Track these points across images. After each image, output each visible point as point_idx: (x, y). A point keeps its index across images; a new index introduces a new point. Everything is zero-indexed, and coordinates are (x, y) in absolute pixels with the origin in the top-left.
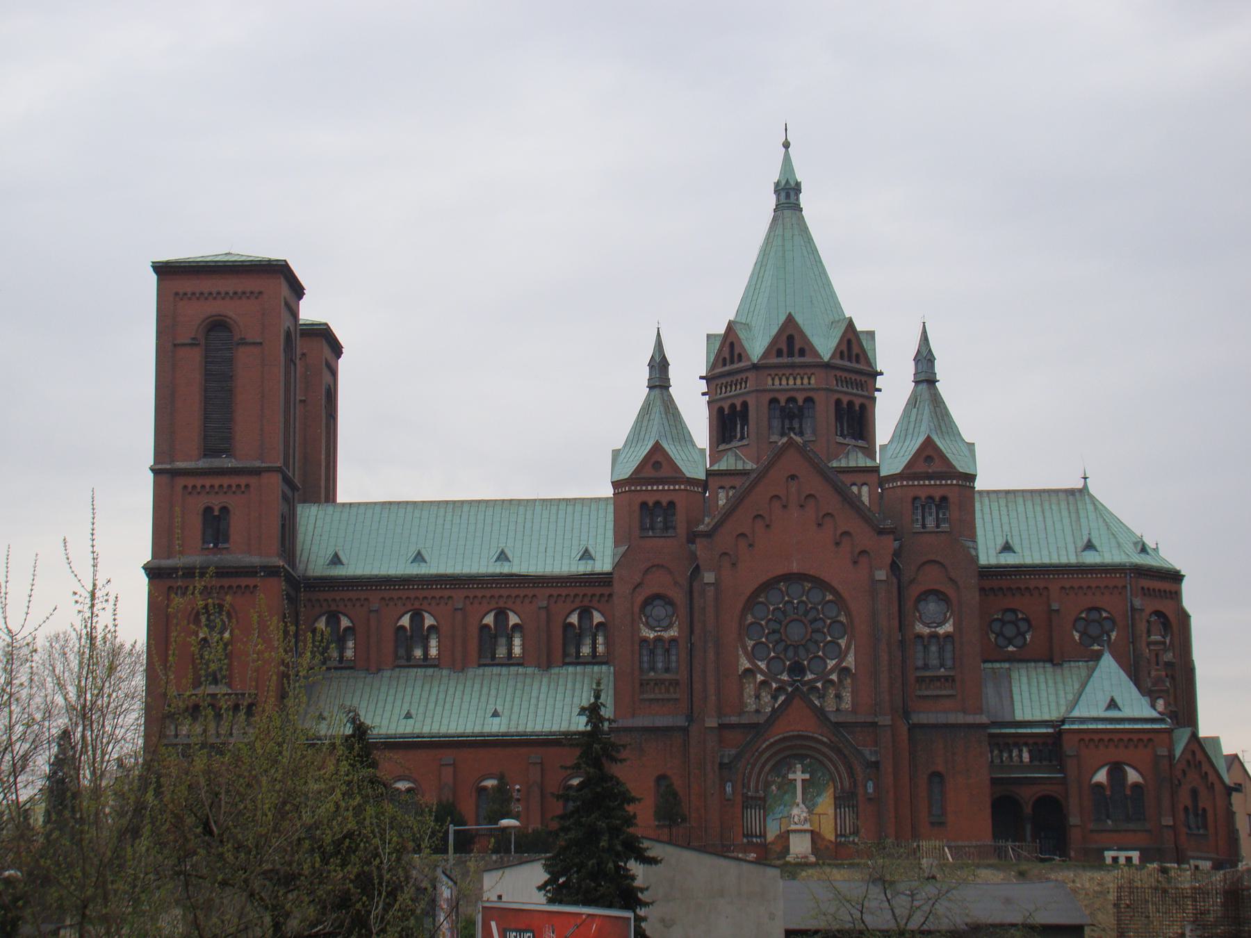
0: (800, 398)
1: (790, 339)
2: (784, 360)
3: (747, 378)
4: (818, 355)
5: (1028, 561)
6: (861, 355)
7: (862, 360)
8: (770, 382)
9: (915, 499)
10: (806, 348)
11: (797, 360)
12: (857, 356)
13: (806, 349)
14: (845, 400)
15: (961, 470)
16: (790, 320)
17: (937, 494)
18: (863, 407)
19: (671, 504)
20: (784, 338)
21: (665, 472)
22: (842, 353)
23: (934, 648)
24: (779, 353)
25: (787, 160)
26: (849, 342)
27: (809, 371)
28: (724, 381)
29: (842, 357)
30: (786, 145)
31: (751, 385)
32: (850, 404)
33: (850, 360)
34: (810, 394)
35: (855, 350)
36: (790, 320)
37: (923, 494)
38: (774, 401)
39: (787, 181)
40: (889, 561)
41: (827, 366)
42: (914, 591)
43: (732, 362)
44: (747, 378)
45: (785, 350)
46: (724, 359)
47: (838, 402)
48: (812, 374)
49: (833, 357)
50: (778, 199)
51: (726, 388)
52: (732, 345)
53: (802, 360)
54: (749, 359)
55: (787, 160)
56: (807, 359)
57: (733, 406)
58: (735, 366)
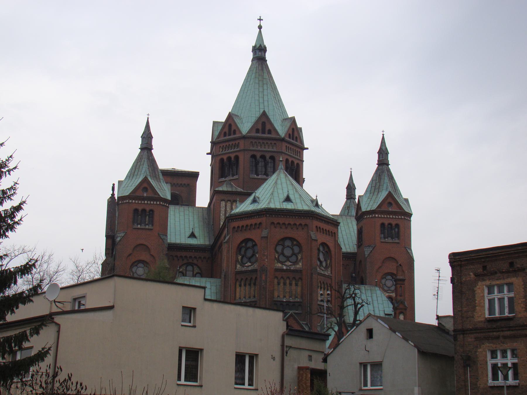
1: (264, 124)
2: (259, 135)
3: (239, 143)
6: (298, 138)
7: (298, 140)
11: (266, 135)
12: (296, 138)
13: (272, 130)
14: (290, 160)
16: (264, 114)
18: (298, 164)
22: (289, 135)
24: (257, 131)
26: (293, 129)
28: (224, 144)
29: (290, 138)
30: (260, 27)
31: (242, 147)
32: (292, 162)
33: (293, 139)
35: (296, 134)
36: (264, 114)
38: (253, 156)
39: (260, 46)
41: (283, 140)
43: (230, 135)
44: (239, 143)
46: (225, 133)
48: (275, 144)
49: (286, 135)
51: (223, 149)
52: (230, 126)
53: (269, 136)
54: (240, 132)
56: (273, 136)
57: (229, 159)
58: (232, 136)
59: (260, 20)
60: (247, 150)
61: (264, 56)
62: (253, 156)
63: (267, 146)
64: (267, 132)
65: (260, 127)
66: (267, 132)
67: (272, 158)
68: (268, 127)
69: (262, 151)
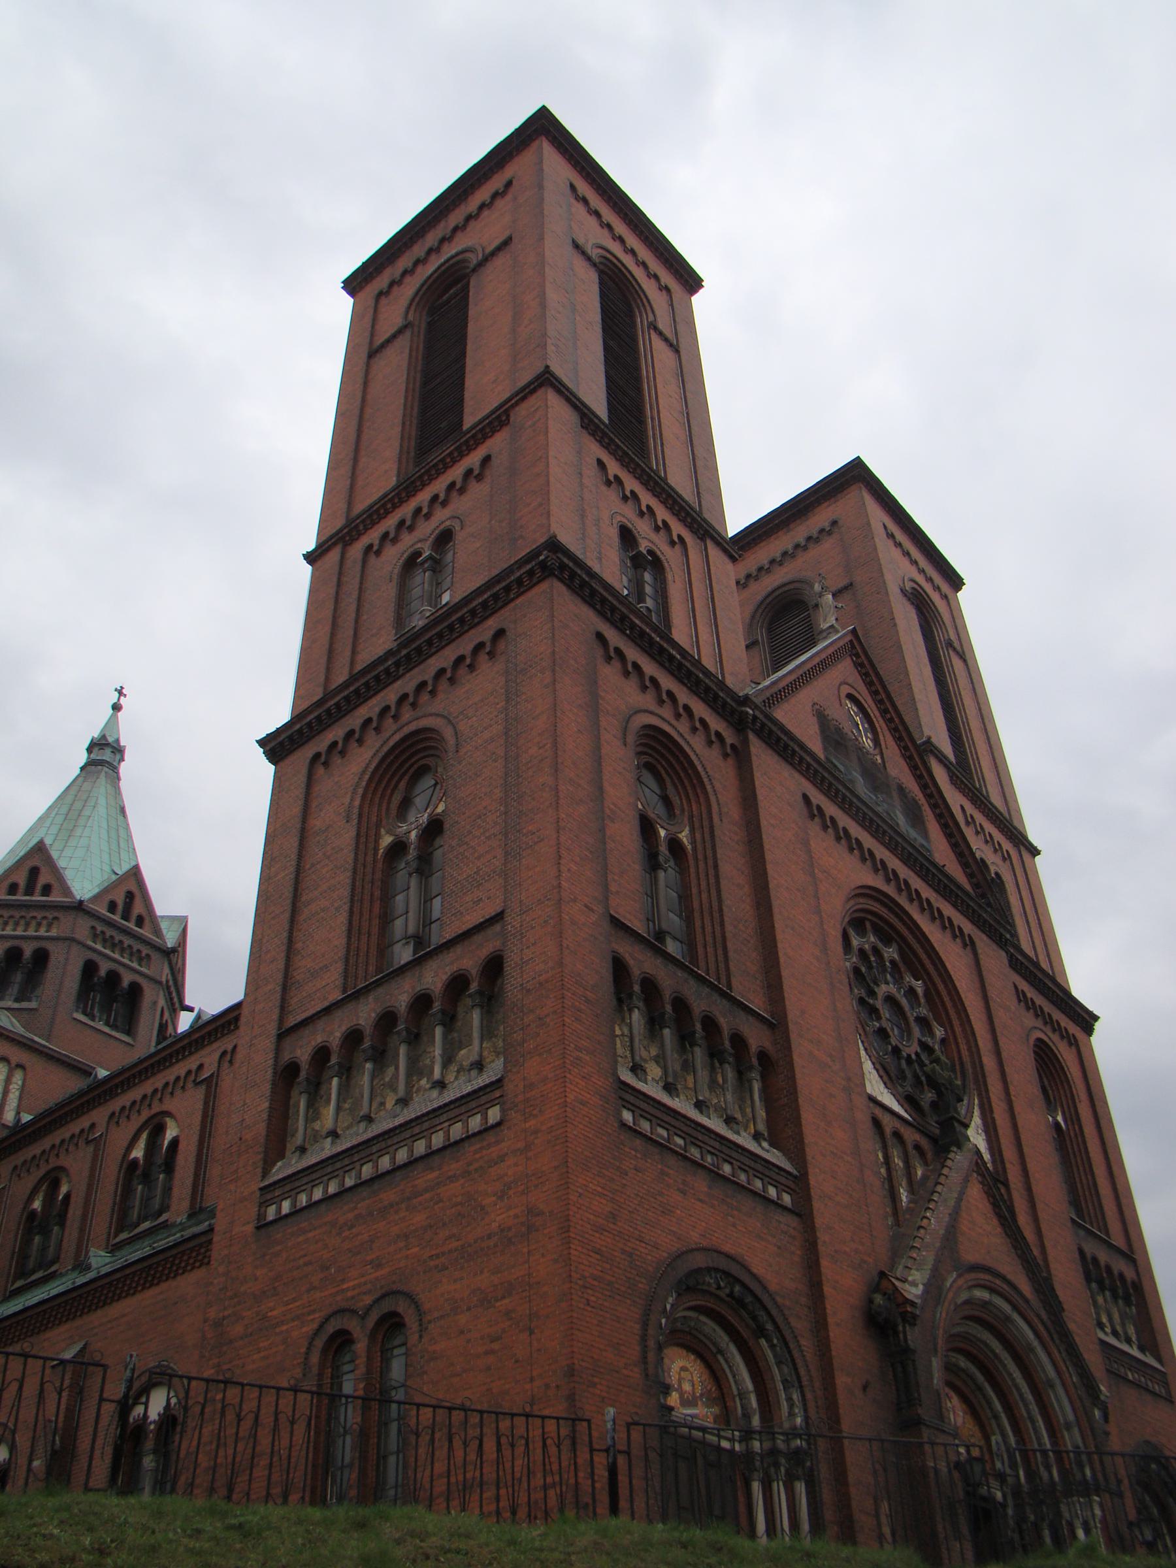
0: (28, 950)
1: (34, 872)
2: (20, 897)
4: (67, 891)
11: (38, 898)
14: (104, 968)
24: (13, 889)
25: (112, 722)
27: (50, 915)
30: (117, 707)
34: (44, 944)
35: (138, 909)
39: (104, 737)
41: (79, 907)
47: (90, 968)
48: (56, 918)
49: (96, 898)
50: (88, 758)
55: (112, 722)
56: (55, 897)
59: (120, 692)
65: (21, 879)
67: (41, 958)
68: (42, 880)
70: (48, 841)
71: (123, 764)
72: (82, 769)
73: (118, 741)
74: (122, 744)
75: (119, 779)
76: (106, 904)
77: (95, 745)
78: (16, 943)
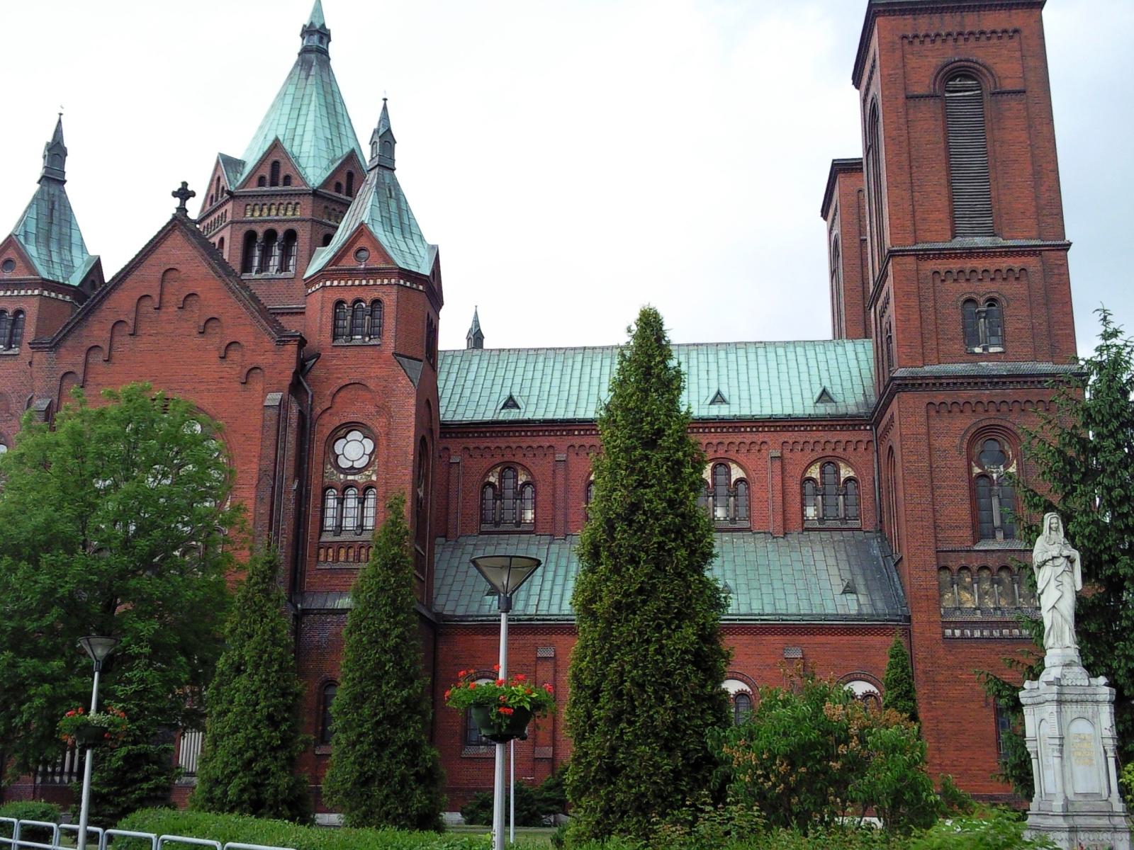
1: (276, 165)
4: (303, 180)
5: (529, 416)
8: (249, 214)
9: (339, 303)
10: (292, 174)
15: (402, 266)
16: (276, 144)
17: (369, 296)
19: (19, 312)
20: (269, 162)
21: (19, 274)
23: (351, 503)
24: (261, 181)
29: (338, 187)
37: (349, 297)
39: (312, 24)
40: (288, 378)
42: (329, 423)
45: (268, 177)
46: (212, 197)
48: (297, 204)
49: (326, 183)
60: (237, 222)
61: (325, 47)
62: (250, 237)
63: (274, 212)
64: (281, 181)
66: (281, 181)
67: (291, 236)
69: (265, 221)
70: (281, 138)
71: (330, 44)
72: (299, 54)
73: (323, 25)
74: (327, 27)
75: (329, 59)
76: (333, 188)
77: (307, 31)
78: (270, 226)
